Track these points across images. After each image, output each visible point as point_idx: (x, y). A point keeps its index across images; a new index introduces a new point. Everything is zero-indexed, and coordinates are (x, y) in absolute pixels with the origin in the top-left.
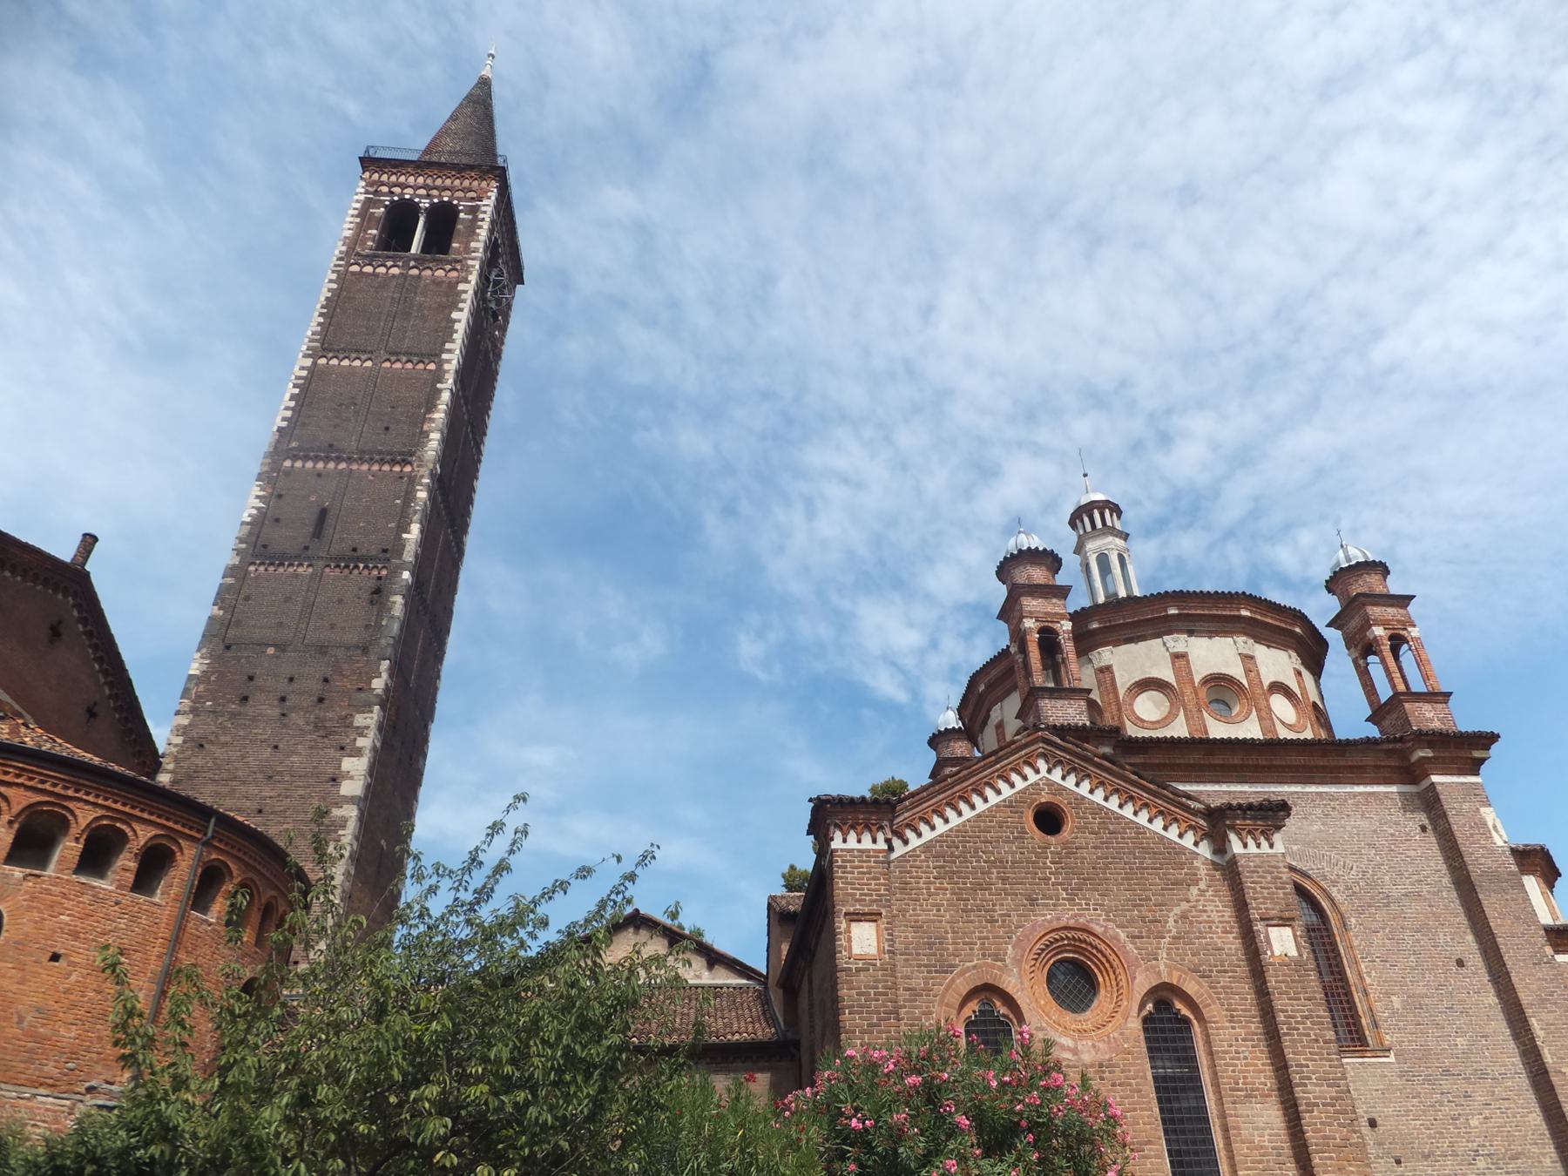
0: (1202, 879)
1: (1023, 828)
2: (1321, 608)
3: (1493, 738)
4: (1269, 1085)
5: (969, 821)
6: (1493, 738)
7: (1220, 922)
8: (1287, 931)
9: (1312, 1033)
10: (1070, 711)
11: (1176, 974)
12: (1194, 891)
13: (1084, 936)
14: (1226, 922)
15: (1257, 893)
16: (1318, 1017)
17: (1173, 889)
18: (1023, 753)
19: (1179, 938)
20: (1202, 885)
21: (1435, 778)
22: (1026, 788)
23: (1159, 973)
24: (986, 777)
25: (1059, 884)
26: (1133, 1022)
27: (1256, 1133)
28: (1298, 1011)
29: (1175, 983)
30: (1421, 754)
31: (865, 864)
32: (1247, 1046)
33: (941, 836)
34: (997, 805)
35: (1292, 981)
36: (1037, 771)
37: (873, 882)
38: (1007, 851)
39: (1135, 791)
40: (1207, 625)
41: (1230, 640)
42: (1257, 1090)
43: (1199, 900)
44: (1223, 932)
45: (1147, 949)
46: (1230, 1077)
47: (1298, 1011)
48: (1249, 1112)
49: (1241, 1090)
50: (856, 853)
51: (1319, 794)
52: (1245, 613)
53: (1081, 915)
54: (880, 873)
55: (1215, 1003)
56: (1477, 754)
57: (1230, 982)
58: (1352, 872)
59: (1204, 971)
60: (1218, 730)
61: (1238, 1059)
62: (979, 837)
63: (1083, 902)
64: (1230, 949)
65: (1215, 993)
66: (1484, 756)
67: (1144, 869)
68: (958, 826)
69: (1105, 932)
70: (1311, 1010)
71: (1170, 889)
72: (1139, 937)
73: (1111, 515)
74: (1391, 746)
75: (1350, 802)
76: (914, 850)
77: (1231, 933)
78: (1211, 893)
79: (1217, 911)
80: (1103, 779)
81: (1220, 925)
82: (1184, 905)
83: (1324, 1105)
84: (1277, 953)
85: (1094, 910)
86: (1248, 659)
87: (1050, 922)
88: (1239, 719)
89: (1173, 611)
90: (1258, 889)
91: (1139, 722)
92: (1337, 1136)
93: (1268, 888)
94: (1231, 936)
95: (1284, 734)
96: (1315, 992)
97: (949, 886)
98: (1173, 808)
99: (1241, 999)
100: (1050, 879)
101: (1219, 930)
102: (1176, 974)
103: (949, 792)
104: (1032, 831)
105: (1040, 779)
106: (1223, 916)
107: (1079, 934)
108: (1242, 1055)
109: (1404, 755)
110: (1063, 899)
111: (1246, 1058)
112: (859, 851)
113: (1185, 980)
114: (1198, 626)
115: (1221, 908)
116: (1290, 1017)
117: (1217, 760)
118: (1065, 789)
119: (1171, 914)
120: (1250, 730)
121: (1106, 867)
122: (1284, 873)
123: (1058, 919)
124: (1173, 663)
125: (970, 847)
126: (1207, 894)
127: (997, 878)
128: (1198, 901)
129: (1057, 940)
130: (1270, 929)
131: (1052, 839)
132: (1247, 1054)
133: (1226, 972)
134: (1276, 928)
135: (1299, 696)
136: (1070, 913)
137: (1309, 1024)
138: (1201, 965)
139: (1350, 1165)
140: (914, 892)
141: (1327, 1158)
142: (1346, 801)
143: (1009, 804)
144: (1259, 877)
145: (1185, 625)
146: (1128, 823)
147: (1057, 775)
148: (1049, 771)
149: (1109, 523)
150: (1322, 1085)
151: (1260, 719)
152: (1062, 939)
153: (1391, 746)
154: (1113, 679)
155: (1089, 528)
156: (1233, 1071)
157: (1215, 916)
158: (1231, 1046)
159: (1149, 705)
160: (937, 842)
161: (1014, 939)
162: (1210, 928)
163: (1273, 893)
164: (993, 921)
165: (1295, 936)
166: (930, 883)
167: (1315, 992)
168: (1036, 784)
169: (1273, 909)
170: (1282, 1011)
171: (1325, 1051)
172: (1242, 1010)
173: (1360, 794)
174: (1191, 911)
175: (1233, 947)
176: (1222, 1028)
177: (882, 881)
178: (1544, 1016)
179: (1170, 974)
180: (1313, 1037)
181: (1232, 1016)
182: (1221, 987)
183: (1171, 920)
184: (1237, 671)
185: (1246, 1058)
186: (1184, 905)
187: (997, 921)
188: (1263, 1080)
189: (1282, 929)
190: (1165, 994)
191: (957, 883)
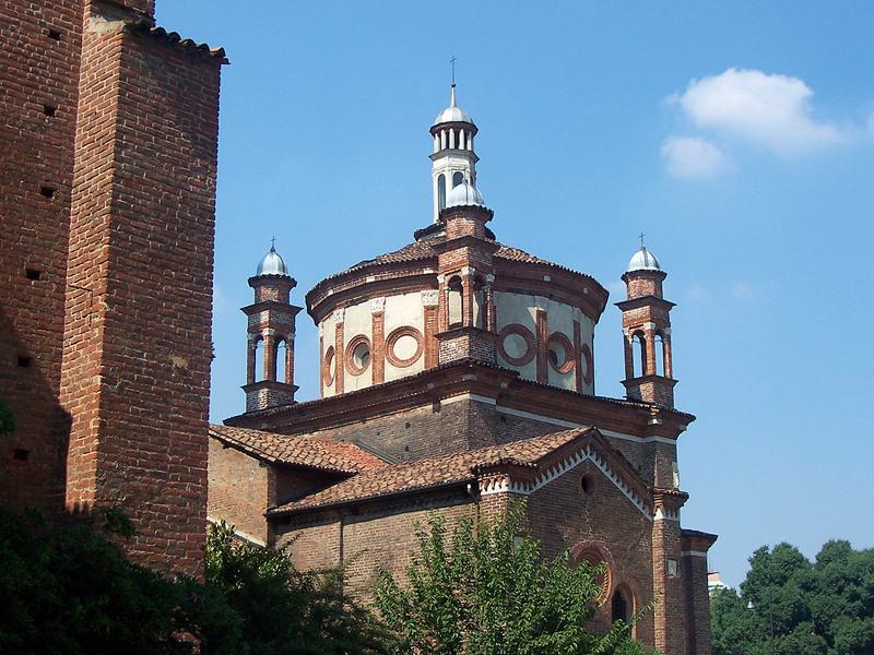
2: (618, 291)
3: (693, 418)
6: (692, 418)
21: (657, 438)
56: (681, 427)
74: (641, 411)
86: (577, 325)
89: (547, 279)
91: (505, 356)
145: (549, 290)
149: (469, 148)
155: (452, 146)
184: (570, 334)
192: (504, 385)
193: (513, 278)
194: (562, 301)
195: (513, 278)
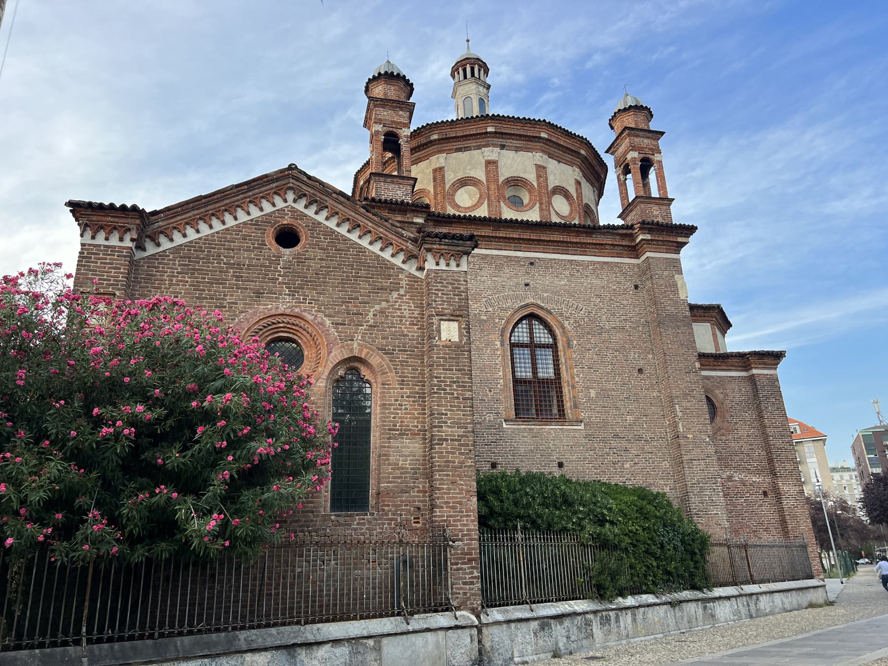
0: (402, 287)
1: (263, 241)
4: (419, 427)
5: (217, 233)
7: (410, 317)
8: (455, 325)
9: (455, 392)
10: (399, 192)
11: (365, 351)
12: (395, 295)
13: (297, 321)
14: (415, 318)
15: (438, 297)
16: (463, 382)
17: (379, 293)
18: (274, 185)
19: (375, 326)
20: (402, 292)
21: (648, 254)
22: (274, 212)
23: (352, 350)
24: (238, 200)
25: (283, 283)
26: (322, 382)
27: (401, 458)
28: (449, 378)
29: (363, 357)
30: (641, 237)
31: (109, 257)
32: (409, 402)
33: (191, 242)
34: (245, 223)
35: (450, 358)
36: (285, 201)
37: (113, 271)
38: (245, 257)
39: (362, 221)
40: (515, 142)
41: (530, 154)
42: (410, 430)
43: (397, 302)
44: (410, 324)
45: (347, 333)
46: (391, 421)
47: (449, 378)
48: (400, 445)
49: (398, 430)
50: (102, 248)
51: (570, 261)
52: (543, 135)
53: (296, 307)
54: (121, 265)
55: (391, 371)
56: (680, 239)
57: (407, 358)
58: (581, 312)
59: (389, 349)
60: (508, 214)
61: (401, 409)
62: (224, 245)
63: (302, 297)
64: (414, 336)
65: (393, 365)
66: (685, 241)
67: (358, 277)
68: (207, 236)
69: (314, 319)
70: (458, 378)
71: (375, 293)
72: (341, 324)
73: (479, 70)
74: (624, 231)
75: (590, 267)
76: (164, 251)
77: (416, 325)
78: (407, 297)
79: (409, 310)
80: (337, 210)
81: (409, 319)
82: (384, 304)
83: (452, 440)
84: (443, 339)
85: (309, 303)
86: (541, 170)
87: (271, 309)
88: (526, 209)
90: (440, 295)
91: (456, 206)
92: (457, 460)
93: (447, 294)
94: (416, 327)
95: (555, 219)
96: (465, 366)
97: (189, 280)
98: (390, 236)
99: (413, 370)
100: (278, 279)
101: (408, 323)
102: (365, 351)
103: (203, 210)
104: (271, 244)
105: (287, 207)
106: (413, 313)
107: (293, 320)
108: (403, 407)
109: (632, 237)
110: (285, 294)
111: (406, 409)
112: (105, 246)
113: (372, 355)
114: (508, 142)
115: (413, 308)
116: (442, 381)
117: (502, 234)
118: (306, 216)
119: (372, 310)
120: (533, 216)
121: (328, 273)
122: (462, 285)
123: (277, 308)
124: (486, 167)
125: (214, 252)
126: (404, 298)
127: (232, 276)
128: (396, 302)
129: (274, 323)
130: (442, 322)
131: (287, 251)
132: (408, 406)
133: (407, 351)
134: (447, 322)
135: (575, 198)
136: (288, 304)
137: (455, 387)
138: (387, 346)
139: (460, 480)
140: (157, 282)
141: (444, 475)
142: (588, 267)
143: (255, 223)
144: (442, 286)
145: (500, 141)
146: (354, 244)
147: (300, 206)
148: (295, 201)
149: (476, 75)
150: (453, 427)
151: (541, 210)
152: (279, 323)
153: (624, 231)
154: (443, 176)
156: (394, 418)
157: (406, 313)
158: (397, 400)
159: (466, 196)
160: (185, 246)
161: (237, 320)
162: (401, 321)
163: (451, 298)
164: (222, 307)
165: (460, 328)
166: (173, 276)
167: (465, 366)
168: (282, 210)
169: (448, 309)
170: (436, 377)
171: (462, 405)
172: (411, 377)
173: (599, 262)
174: (389, 309)
175: (416, 335)
176: (393, 388)
177: (122, 270)
178: (684, 404)
179: (361, 351)
180: (456, 395)
181: (403, 381)
182: (399, 361)
183: (371, 314)
184: (531, 176)
185: (406, 409)
186: (384, 304)
187: (225, 307)
188: (416, 424)
189: (451, 323)
190: (356, 364)
191: (197, 278)
192: (420, 220)
193: (456, 138)
194: (517, 149)
195: (456, 138)
